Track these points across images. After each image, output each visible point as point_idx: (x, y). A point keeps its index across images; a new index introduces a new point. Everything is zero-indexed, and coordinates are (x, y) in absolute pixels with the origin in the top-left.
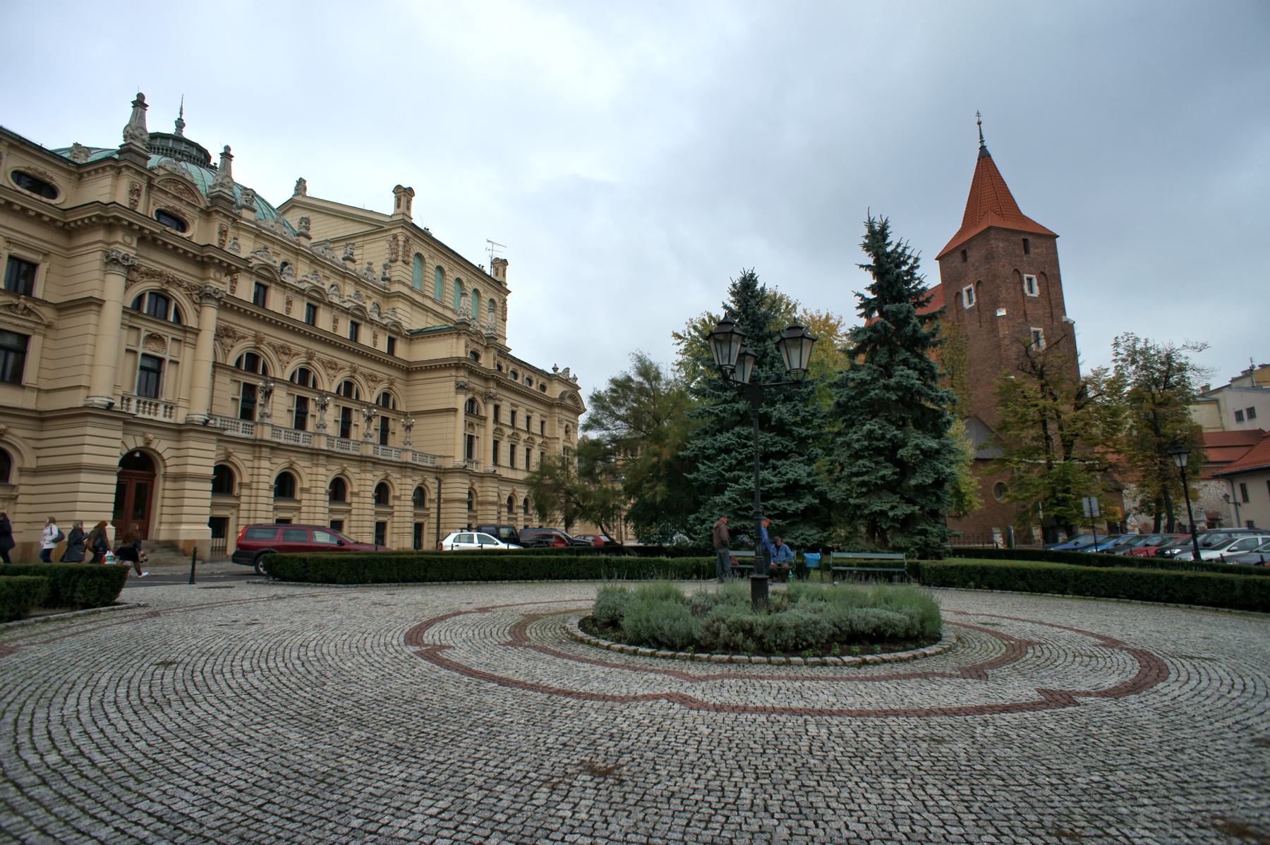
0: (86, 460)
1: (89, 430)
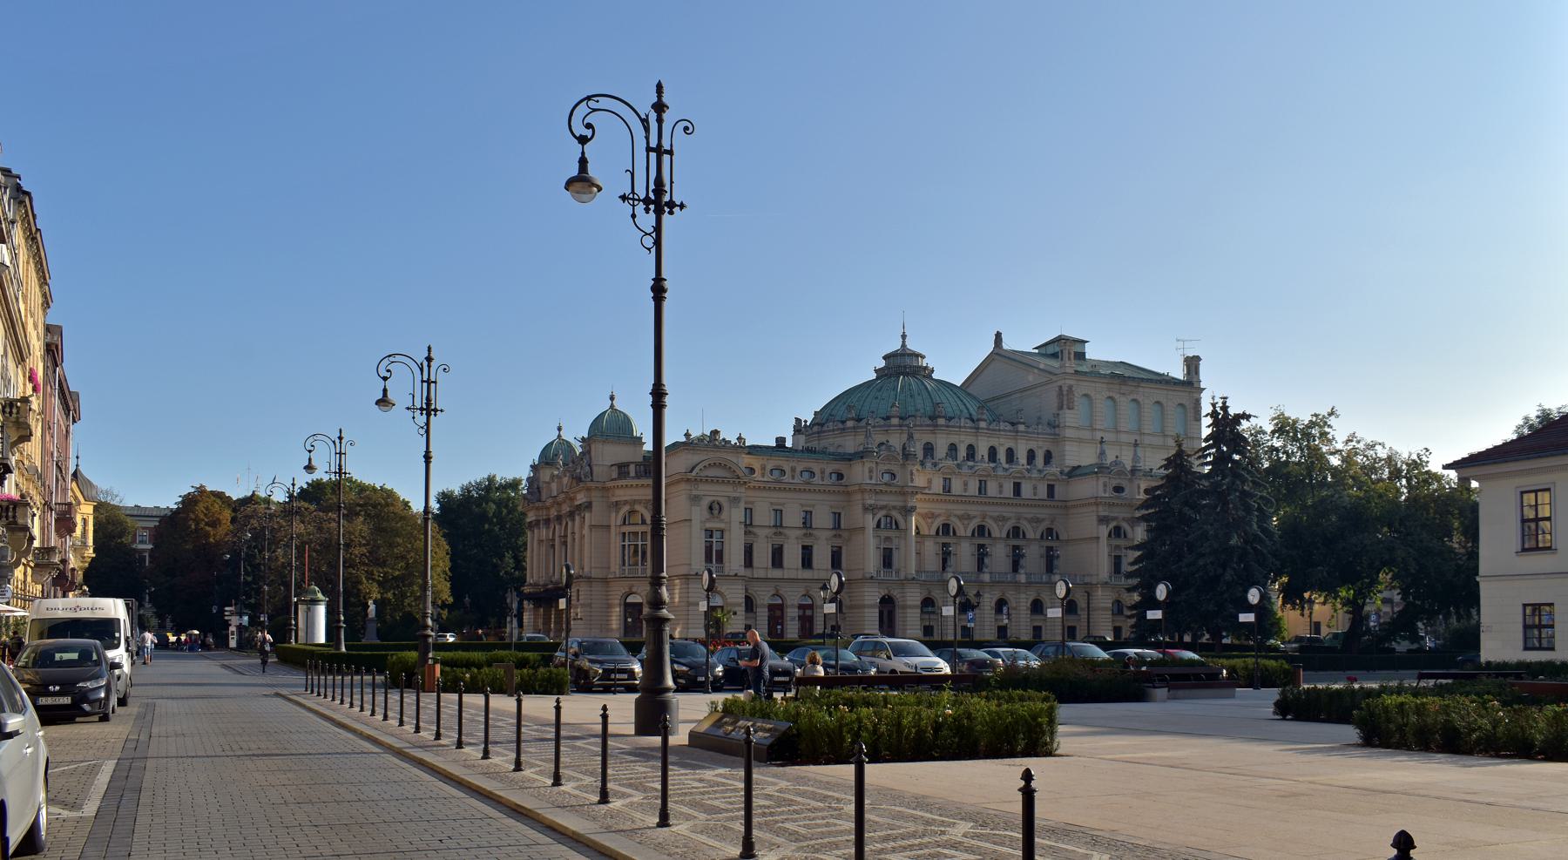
0: (866, 602)
1: (866, 589)
